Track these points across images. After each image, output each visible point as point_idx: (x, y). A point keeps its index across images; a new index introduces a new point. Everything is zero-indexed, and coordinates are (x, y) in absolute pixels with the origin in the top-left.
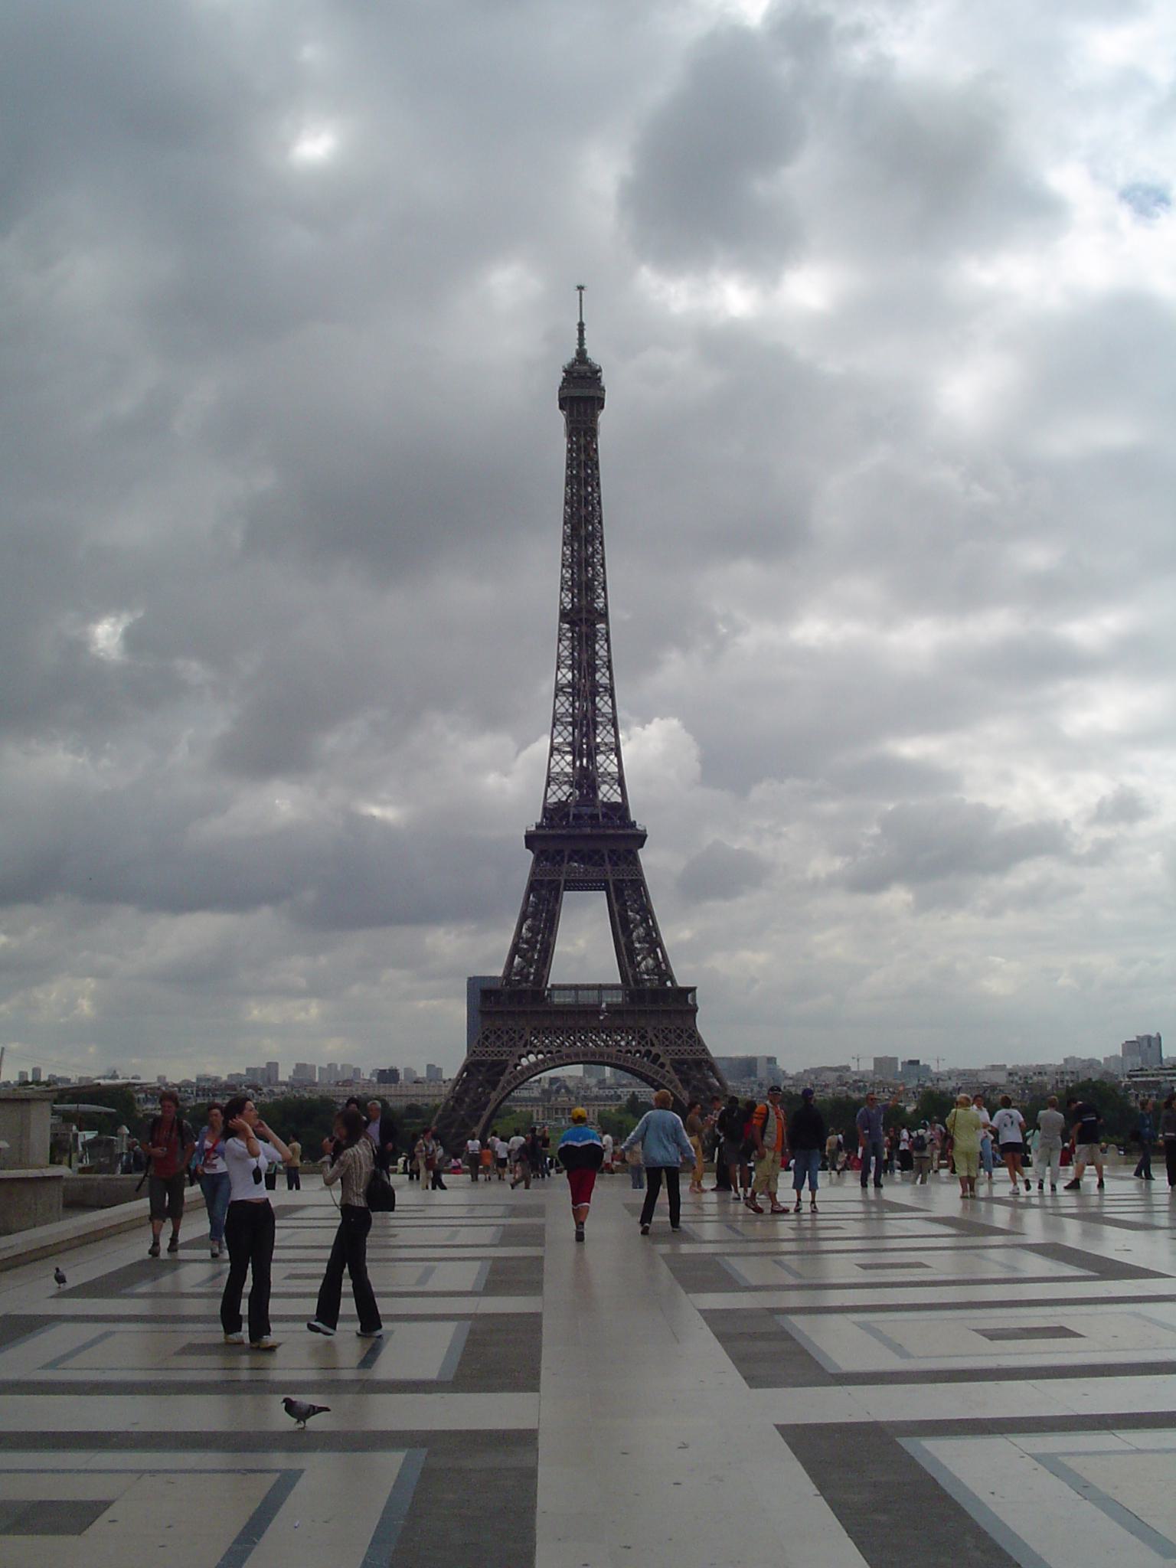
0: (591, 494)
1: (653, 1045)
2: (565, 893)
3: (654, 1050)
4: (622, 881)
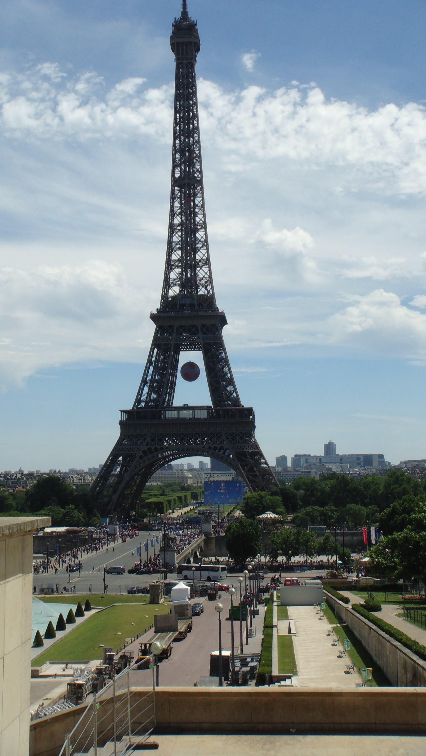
2: (180, 352)
4: (209, 344)
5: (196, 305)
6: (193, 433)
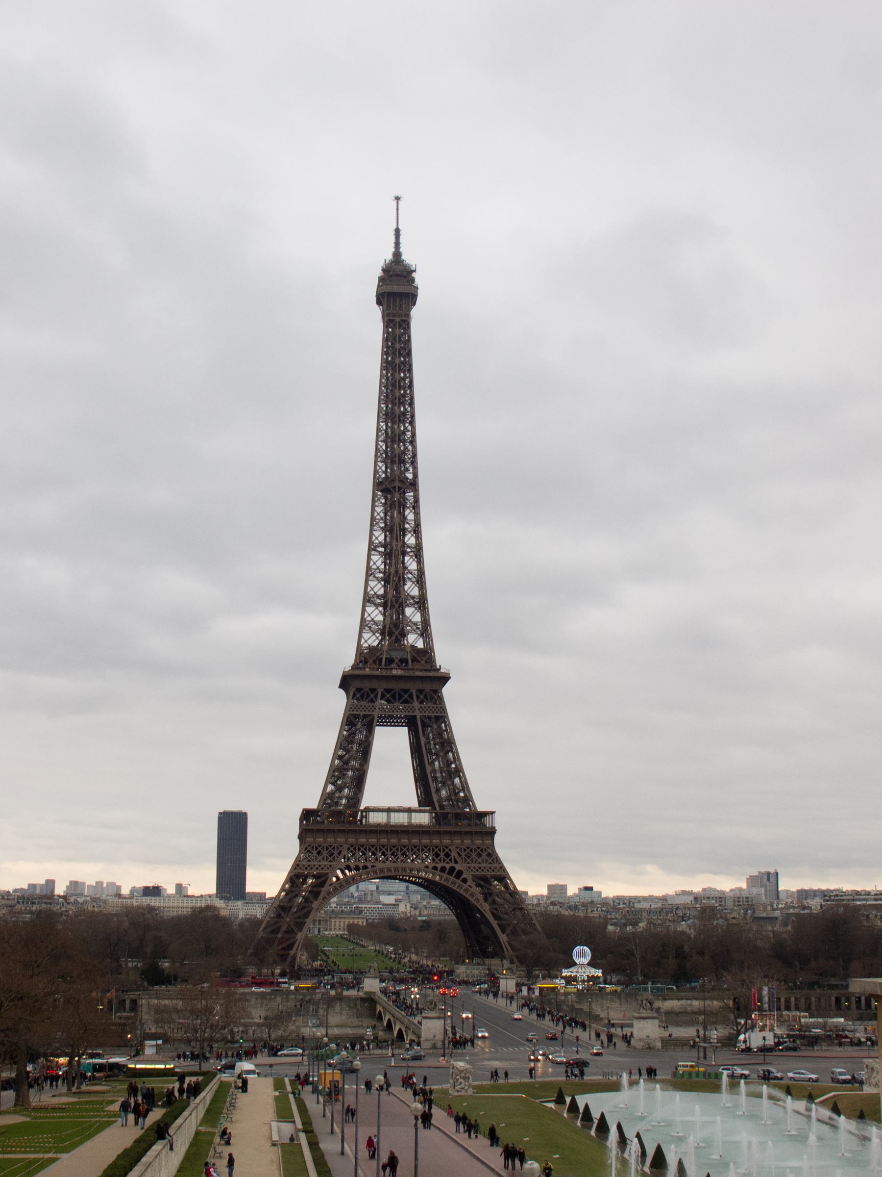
0: (404, 379)
1: (456, 862)
3: (458, 867)
4: (429, 718)
5: (410, 661)
6: (387, 847)
